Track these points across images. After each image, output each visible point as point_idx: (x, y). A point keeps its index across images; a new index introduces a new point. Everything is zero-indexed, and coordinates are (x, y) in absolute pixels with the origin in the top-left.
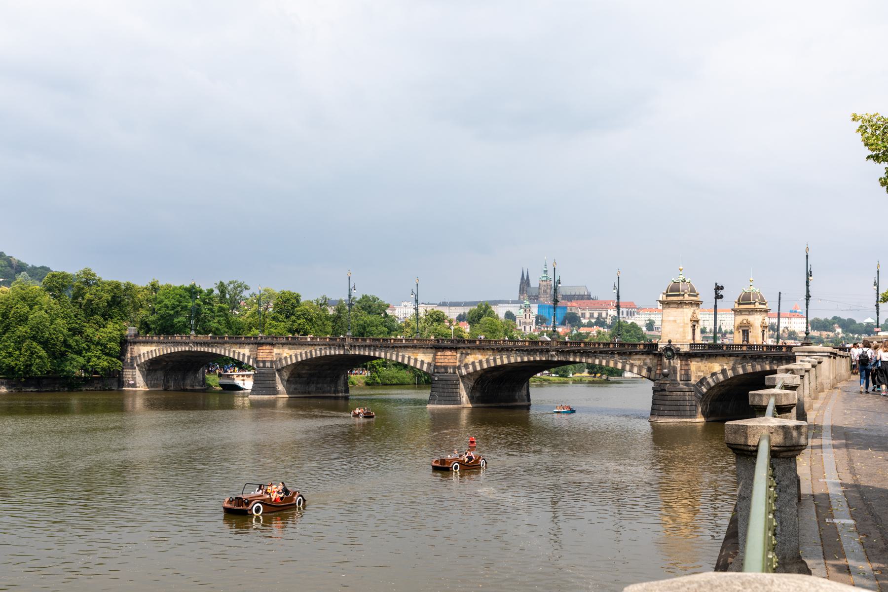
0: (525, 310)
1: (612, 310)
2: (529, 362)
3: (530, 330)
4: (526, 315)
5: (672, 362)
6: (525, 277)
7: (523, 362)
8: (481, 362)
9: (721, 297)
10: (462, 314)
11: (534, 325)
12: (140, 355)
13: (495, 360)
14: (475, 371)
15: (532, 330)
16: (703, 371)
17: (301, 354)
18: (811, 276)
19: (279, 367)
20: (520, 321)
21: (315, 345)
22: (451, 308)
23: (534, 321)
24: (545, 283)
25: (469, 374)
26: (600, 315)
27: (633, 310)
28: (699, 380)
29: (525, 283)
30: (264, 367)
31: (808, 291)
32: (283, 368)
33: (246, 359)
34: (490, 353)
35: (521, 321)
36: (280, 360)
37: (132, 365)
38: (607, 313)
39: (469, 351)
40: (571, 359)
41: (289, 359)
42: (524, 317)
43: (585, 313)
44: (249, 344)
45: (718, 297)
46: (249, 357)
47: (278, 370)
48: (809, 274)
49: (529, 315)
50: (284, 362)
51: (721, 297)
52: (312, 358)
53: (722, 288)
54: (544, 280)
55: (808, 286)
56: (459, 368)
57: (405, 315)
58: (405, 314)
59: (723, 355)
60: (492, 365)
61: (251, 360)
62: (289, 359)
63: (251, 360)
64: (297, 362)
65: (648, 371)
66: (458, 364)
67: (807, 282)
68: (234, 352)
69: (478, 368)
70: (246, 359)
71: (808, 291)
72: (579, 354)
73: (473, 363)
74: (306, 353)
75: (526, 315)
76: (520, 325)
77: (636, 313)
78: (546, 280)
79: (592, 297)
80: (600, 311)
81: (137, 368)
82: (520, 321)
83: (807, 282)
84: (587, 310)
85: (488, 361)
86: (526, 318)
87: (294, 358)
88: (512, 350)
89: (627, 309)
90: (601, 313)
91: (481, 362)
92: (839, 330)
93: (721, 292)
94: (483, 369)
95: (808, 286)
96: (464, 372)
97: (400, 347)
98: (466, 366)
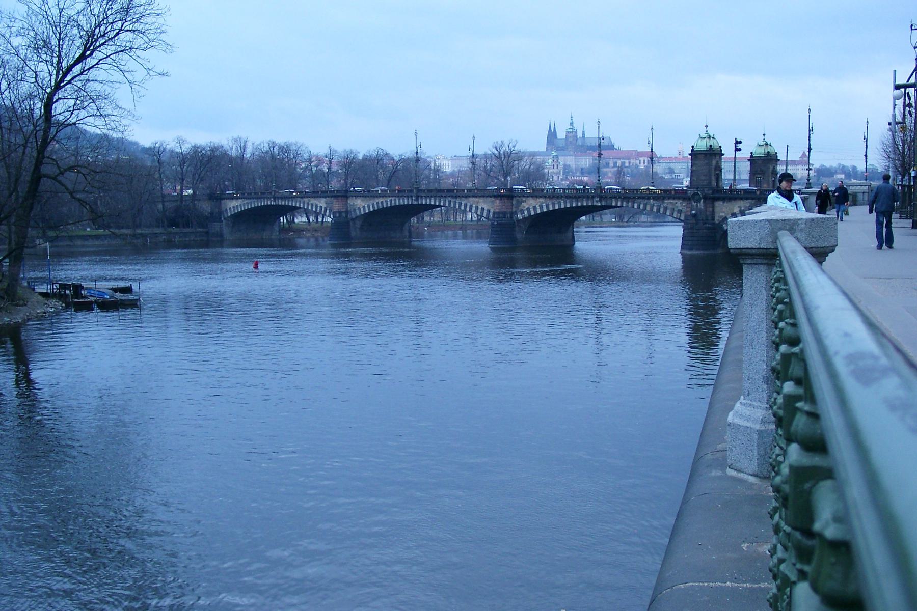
2: (577, 207)
5: (699, 204)
7: (571, 207)
8: (535, 208)
9: (740, 150)
12: (226, 210)
13: (547, 206)
14: (530, 216)
16: (724, 212)
17: (373, 205)
18: (812, 131)
19: (354, 216)
21: (386, 196)
23: (562, 171)
24: (570, 135)
25: (524, 218)
28: (721, 220)
29: (552, 135)
30: (340, 216)
31: (810, 145)
32: (357, 217)
33: (323, 210)
34: (542, 200)
36: (355, 210)
37: (220, 218)
39: (524, 199)
40: (614, 204)
41: (362, 209)
44: (325, 197)
45: (737, 150)
46: (326, 209)
47: (353, 219)
48: (811, 130)
50: (357, 211)
51: (740, 150)
52: (383, 208)
53: (740, 142)
55: (809, 140)
56: (516, 213)
59: (741, 199)
60: (545, 210)
61: (328, 211)
62: (362, 209)
63: (328, 211)
64: (370, 212)
65: (678, 213)
66: (514, 210)
67: (809, 137)
68: (312, 205)
69: (533, 213)
70: (323, 210)
71: (810, 145)
72: (619, 200)
73: (528, 209)
74: (378, 203)
78: (572, 132)
79: (615, 147)
81: (224, 221)
83: (809, 137)
85: (541, 207)
87: (367, 208)
88: (562, 197)
90: (624, 163)
91: (535, 208)
93: (739, 146)
94: (536, 215)
95: (809, 140)
96: (520, 217)
97: (463, 196)
98: (522, 212)
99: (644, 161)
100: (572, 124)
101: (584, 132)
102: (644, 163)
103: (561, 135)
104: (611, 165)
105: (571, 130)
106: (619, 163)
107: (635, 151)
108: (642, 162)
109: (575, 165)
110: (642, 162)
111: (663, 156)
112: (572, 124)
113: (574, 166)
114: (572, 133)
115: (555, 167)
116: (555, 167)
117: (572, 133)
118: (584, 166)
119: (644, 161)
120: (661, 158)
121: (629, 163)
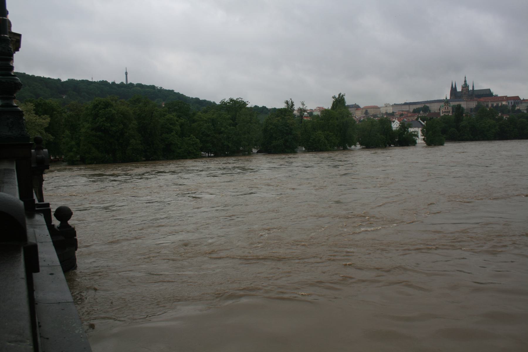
0: (445, 104)
1: (505, 102)
4: (445, 107)
11: (451, 112)
20: (442, 111)
22: (410, 106)
23: (451, 111)
24: (465, 89)
26: (498, 105)
27: (518, 101)
29: (453, 90)
38: (502, 104)
42: (444, 109)
43: (488, 105)
49: (448, 107)
57: (386, 111)
75: (445, 107)
76: (442, 114)
77: (520, 103)
78: (466, 87)
79: (494, 94)
80: (492, 103)
82: (442, 111)
84: (490, 103)
86: (445, 109)
89: (515, 101)
90: (498, 104)
99: (511, 102)
100: (465, 81)
101: (473, 86)
102: (511, 104)
103: (459, 89)
105: (465, 86)
106: (495, 105)
107: (506, 97)
109: (466, 107)
111: (525, 99)
112: (465, 81)
113: (466, 107)
114: (465, 86)
115: (446, 108)
116: (446, 108)
117: (465, 86)
118: (472, 107)
119: (511, 102)
120: (524, 100)
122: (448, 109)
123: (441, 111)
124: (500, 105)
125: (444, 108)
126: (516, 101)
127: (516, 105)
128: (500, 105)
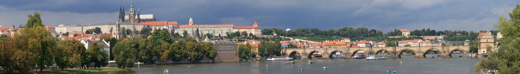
1: (166, 26)
3: (120, 37)
4: (117, 29)
6: (122, 11)
10: (88, 30)
15: (120, 37)
20: (114, 33)
23: (122, 32)
35: (115, 32)
38: (163, 28)
54: (132, 12)
58: (61, 31)
75: (117, 29)
76: (114, 35)
82: (114, 33)
84: (153, 26)
86: (117, 31)
90: (160, 28)
92: (275, 34)
99: (171, 27)
102: (171, 28)
104: (153, 29)
106: (158, 28)
108: (170, 28)
110: (170, 28)
121: (163, 28)
122: (119, 31)
123: (113, 32)
124: (162, 29)
125: (116, 30)
126: (175, 26)
127: (175, 30)
128: (162, 29)
